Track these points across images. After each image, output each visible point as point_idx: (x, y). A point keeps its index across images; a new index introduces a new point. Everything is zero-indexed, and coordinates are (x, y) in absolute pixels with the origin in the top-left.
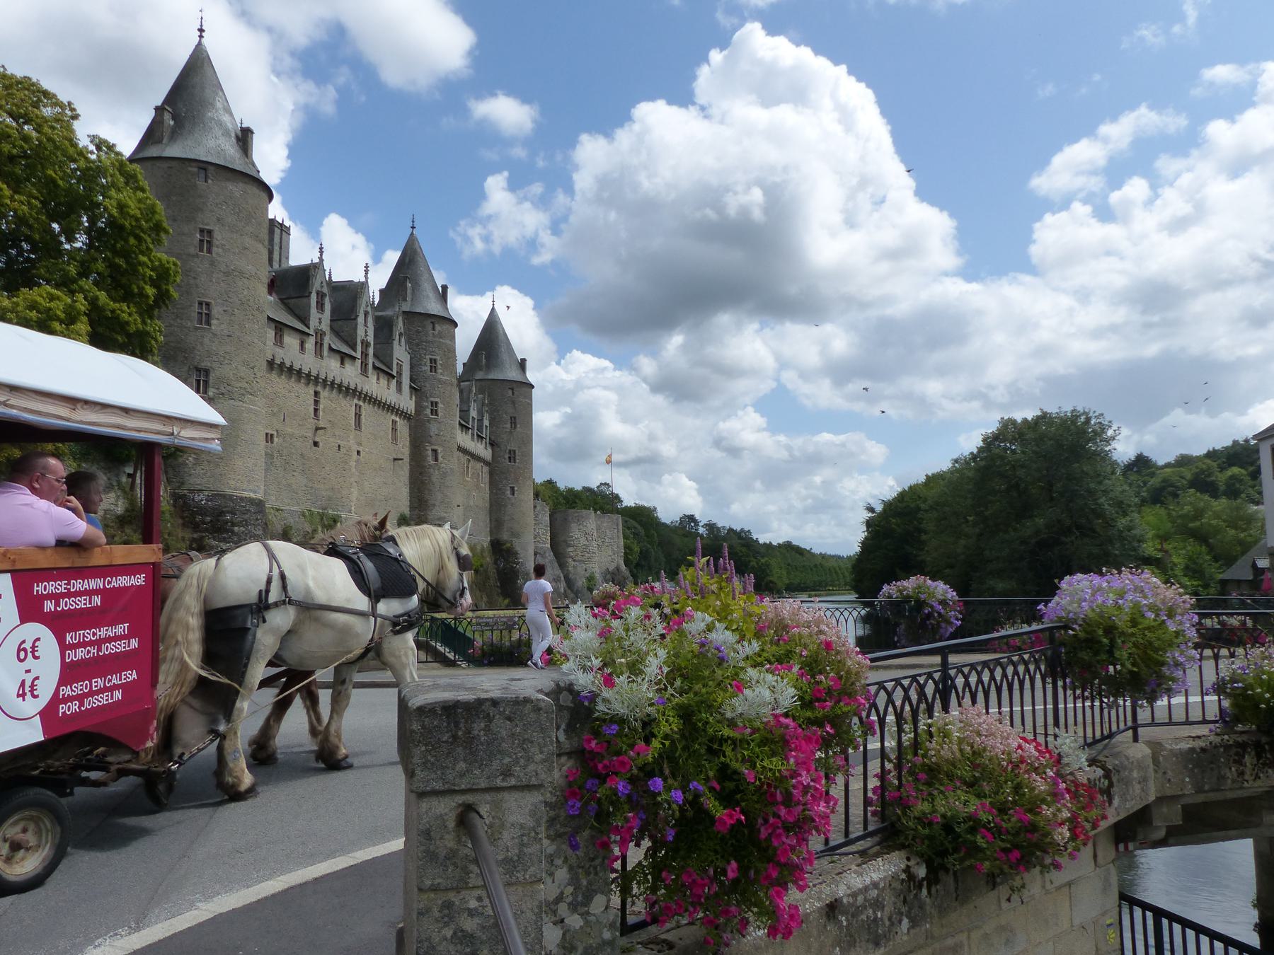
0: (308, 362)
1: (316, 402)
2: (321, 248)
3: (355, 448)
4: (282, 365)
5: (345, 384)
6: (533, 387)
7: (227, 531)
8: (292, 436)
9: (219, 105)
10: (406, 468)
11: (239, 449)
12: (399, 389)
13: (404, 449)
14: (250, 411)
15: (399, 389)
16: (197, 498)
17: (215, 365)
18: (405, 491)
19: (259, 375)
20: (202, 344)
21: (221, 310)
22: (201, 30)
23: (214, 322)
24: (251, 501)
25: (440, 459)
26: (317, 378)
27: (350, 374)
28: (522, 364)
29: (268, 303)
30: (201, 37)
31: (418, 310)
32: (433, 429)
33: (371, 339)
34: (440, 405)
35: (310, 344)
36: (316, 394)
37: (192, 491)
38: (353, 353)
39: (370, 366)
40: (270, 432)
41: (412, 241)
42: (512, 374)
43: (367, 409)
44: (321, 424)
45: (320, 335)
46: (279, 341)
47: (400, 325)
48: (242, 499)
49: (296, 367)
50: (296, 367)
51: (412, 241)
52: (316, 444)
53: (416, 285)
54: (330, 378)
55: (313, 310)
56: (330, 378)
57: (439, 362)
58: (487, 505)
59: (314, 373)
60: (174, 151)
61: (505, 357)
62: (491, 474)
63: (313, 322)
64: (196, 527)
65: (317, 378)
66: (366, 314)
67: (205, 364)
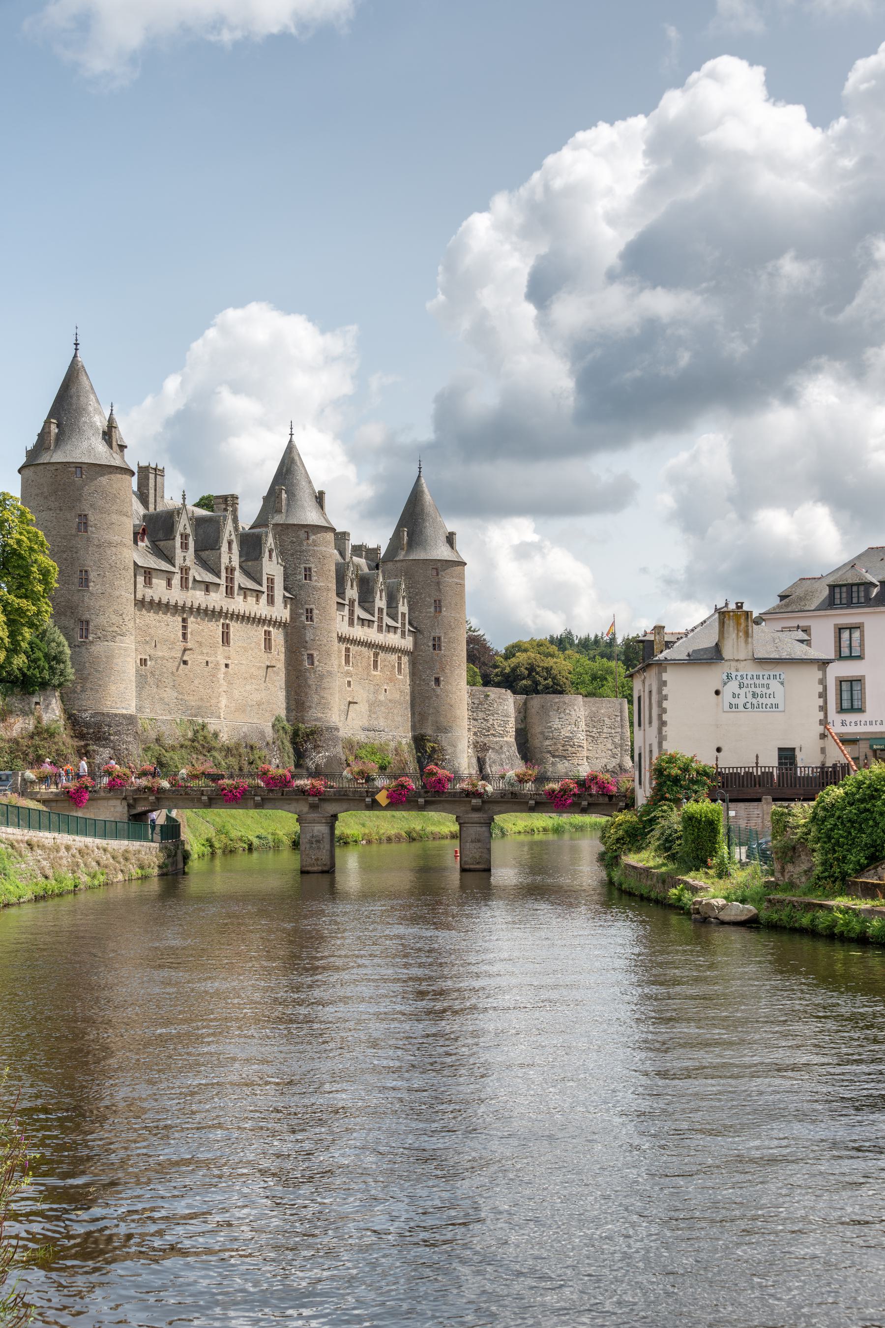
0: (176, 595)
1: (185, 627)
2: (184, 495)
4: (152, 601)
5: (211, 608)
6: (465, 564)
8: (163, 658)
9: (91, 409)
11: (113, 678)
12: (271, 601)
14: (120, 648)
15: (271, 601)
16: (84, 716)
17: (93, 617)
18: (281, 695)
19: (127, 619)
20: (83, 601)
21: (95, 574)
23: (92, 584)
24: (124, 716)
25: (316, 663)
27: (216, 599)
29: (140, 555)
30: (76, 349)
31: (291, 522)
32: (309, 636)
33: (236, 563)
34: (315, 611)
35: (176, 580)
36: (184, 620)
37: (79, 711)
38: (217, 580)
40: (144, 657)
42: (442, 552)
44: (189, 645)
45: (185, 570)
46: (148, 583)
47: (270, 542)
48: (116, 715)
49: (164, 601)
50: (164, 601)
52: (185, 663)
53: (291, 495)
55: (178, 551)
56: (196, 605)
57: (314, 570)
58: (408, 698)
59: (180, 603)
60: (58, 457)
61: (429, 531)
62: (413, 664)
63: (179, 561)
64: (81, 736)
65: (184, 607)
66: (230, 543)
67: (86, 616)
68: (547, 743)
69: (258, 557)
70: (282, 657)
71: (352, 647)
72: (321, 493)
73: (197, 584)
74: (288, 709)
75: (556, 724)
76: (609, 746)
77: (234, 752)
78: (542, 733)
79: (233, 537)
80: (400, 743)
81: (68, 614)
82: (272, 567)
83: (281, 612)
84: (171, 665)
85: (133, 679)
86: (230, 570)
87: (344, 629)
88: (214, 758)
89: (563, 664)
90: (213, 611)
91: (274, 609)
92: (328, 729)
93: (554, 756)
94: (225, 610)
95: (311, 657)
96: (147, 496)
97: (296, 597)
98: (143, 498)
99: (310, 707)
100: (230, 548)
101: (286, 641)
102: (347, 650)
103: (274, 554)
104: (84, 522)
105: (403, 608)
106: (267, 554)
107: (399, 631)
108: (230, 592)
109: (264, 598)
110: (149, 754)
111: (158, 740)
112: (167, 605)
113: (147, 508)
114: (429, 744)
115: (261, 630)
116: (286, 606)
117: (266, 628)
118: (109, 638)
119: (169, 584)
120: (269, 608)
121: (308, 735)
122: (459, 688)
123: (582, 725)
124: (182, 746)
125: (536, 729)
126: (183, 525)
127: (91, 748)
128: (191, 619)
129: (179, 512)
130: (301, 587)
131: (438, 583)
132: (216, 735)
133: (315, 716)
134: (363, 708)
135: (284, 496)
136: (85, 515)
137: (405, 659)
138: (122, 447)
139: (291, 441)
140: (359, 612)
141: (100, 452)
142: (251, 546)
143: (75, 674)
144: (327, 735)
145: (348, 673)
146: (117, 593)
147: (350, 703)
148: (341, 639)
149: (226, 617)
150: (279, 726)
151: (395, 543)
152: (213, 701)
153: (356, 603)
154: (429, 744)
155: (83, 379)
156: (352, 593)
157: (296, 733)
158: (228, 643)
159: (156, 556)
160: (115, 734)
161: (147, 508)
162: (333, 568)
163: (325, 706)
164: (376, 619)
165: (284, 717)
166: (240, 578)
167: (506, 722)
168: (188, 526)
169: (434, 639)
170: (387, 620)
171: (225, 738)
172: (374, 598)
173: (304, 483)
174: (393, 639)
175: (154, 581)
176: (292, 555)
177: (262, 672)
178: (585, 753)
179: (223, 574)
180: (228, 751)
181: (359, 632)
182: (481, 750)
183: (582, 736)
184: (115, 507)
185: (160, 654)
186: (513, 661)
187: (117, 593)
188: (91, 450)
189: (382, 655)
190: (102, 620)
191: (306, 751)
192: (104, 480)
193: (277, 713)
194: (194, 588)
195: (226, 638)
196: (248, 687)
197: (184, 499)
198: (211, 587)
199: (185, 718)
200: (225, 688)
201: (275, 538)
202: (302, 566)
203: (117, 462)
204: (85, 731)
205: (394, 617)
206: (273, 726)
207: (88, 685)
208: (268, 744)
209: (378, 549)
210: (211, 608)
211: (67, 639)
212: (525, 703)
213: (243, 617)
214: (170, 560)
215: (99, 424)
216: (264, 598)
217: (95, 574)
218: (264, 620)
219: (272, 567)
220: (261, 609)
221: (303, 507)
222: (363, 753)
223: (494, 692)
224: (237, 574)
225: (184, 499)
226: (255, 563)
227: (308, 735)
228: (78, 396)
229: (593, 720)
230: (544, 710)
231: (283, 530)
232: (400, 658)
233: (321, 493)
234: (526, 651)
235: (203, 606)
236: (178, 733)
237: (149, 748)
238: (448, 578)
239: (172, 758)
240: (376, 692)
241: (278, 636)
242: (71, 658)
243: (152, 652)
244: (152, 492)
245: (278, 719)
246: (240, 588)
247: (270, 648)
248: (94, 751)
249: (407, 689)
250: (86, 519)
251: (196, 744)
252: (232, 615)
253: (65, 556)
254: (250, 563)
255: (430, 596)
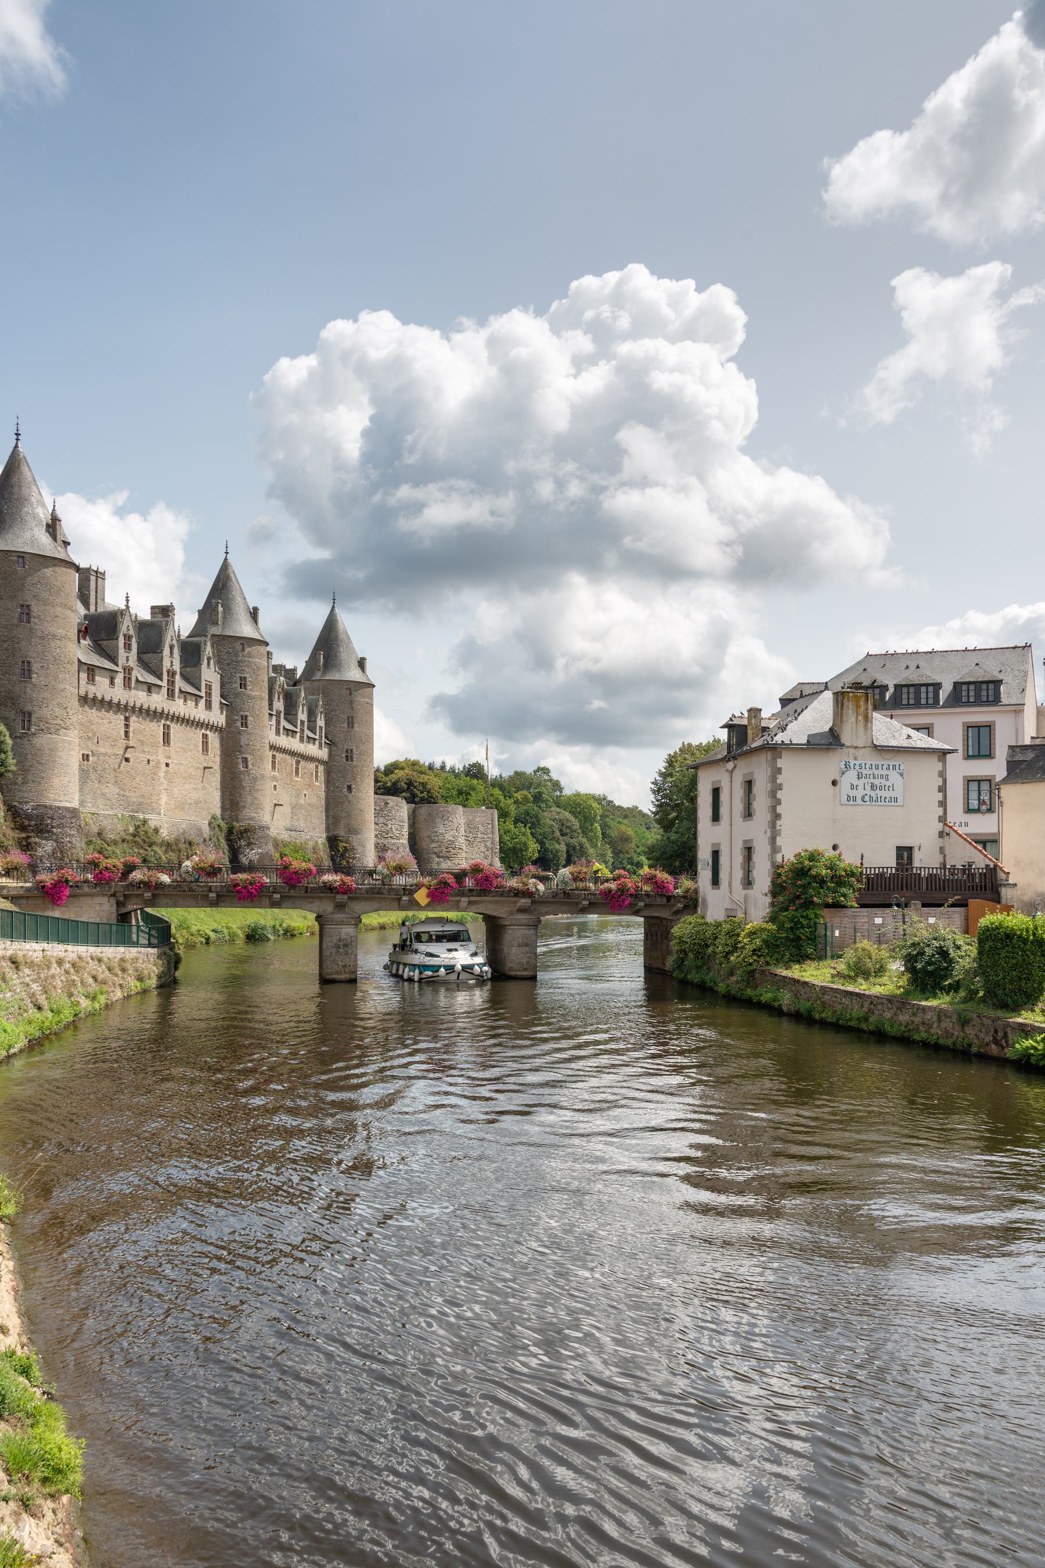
0: (118, 693)
1: (127, 726)
3: (164, 761)
4: (95, 699)
5: (153, 708)
7: (49, 832)
8: (105, 754)
9: (33, 500)
10: (218, 776)
11: (56, 771)
12: (209, 706)
13: (215, 757)
14: (64, 741)
15: (209, 706)
16: (25, 808)
17: (36, 708)
18: (217, 795)
19: (71, 713)
22: (17, 434)
23: (34, 676)
24: (67, 809)
25: (250, 766)
26: (126, 706)
27: (157, 701)
28: (362, 663)
29: (82, 651)
32: (244, 740)
33: (177, 667)
34: (250, 718)
35: (119, 679)
36: (127, 719)
37: (20, 803)
38: (159, 682)
39: (177, 691)
40: (86, 753)
41: (225, 566)
42: (354, 674)
43: (175, 729)
44: (131, 743)
45: (128, 670)
46: (91, 679)
47: (208, 650)
48: (59, 808)
51: (225, 566)
52: (127, 760)
54: (138, 705)
55: (121, 650)
56: (138, 705)
58: (323, 802)
61: (343, 655)
62: (328, 773)
63: (122, 661)
64: (23, 828)
65: (126, 706)
66: (171, 647)
67: (29, 708)
68: (434, 845)
69: (198, 663)
70: (218, 759)
71: (277, 754)
72: (256, 609)
73: (140, 685)
74: (223, 808)
75: (441, 829)
76: (483, 849)
77: (174, 847)
78: (429, 837)
79: (175, 642)
80: (317, 842)
81: (9, 704)
82: (210, 674)
83: (218, 717)
84: (114, 762)
85: (77, 772)
86: (172, 674)
87: (272, 737)
88: (155, 852)
89: (434, 783)
90: (155, 712)
91: (212, 714)
92: (260, 827)
93: (439, 857)
94: (166, 712)
95: (245, 761)
96: (88, 597)
97: (230, 705)
98: (84, 599)
99: (244, 807)
100: (171, 653)
101: (222, 745)
102: (274, 757)
103: (212, 662)
104: (26, 612)
105: (321, 722)
106: (205, 661)
107: (317, 742)
108: (171, 694)
109: (202, 702)
110: (91, 847)
111: (99, 834)
112: (110, 702)
113: (88, 608)
114: (341, 844)
115: (200, 732)
116: (222, 713)
117: (203, 731)
118: (52, 731)
119: (112, 683)
120: (207, 713)
121: (242, 833)
122: (367, 796)
123: (462, 830)
124: (123, 841)
125: (424, 834)
126: (125, 627)
127: (33, 840)
128: (133, 718)
129: (122, 613)
130: (237, 695)
131: (351, 702)
132: (156, 830)
133: (249, 815)
134: (288, 812)
135: (220, 609)
136: (28, 606)
137: (321, 768)
138: (66, 544)
139: (226, 559)
140: (284, 723)
141: (44, 544)
142: (191, 652)
143: (16, 765)
144: (259, 833)
145: (274, 778)
146: (61, 686)
147: (276, 805)
148: (272, 747)
149: (167, 719)
150: (215, 824)
151: (312, 665)
152: (154, 798)
153: (282, 715)
154: (341, 844)
155: (24, 469)
156: (279, 705)
157: (230, 831)
158: (169, 743)
159: (99, 655)
160: (58, 827)
161: (88, 608)
162: (266, 679)
163: (259, 807)
164: (298, 730)
165: (219, 816)
166: (179, 683)
167: (402, 827)
168: (131, 627)
169: (347, 751)
170: (307, 732)
171: (164, 833)
172: (297, 711)
173: (239, 599)
174: (312, 750)
175: (97, 678)
176: (228, 664)
177: (200, 773)
178: (464, 855)
179: (165, 677)
180: (168, 846)
181: (284, 741)
182: (381, 849)
183: (462, 840)
184: (59, 600)
185: (103, 750)
186: (393, 777)
187: (61, 686)
188: (33, 541)
189: (302, 763)
190: (45, 712)
191: (240, 847)
192: (48, 572)
193: (213, 812)
194: (136, 689)
195: (166, 739)
196: (187, 787)
197: (127, 601)
198: (153, 689)
199: (127, 814)
200: (165, 786)
201: (213, 647)
202: (238, 675)
203: (62, 556)
204: (26, 823)
205: (312, 729)
206: (210, 824)
207: (30, 777)
208: (205, 840)
209: (295, 670)
210: (153, 708)
211: (8, 729)
212: (414, 811)
213: (183, 719)
214: (114, 660)
215: (42, 516)
216: (202, 702)
217: (38, 665)
218: (203, 724)
219: (210, 674)
220: (199, 712)
221: (238, 620)
222: (287, 851)
223: (392, 800)
224: (178, 677)
225: (127, 601)
226: (194, 669)
227: (242, 833)
228: (20, 487)
229: (470, 826)
230: (431, 818)
231: (220, 640)
232: (317, 767)
233: (256, 609)
234: (402, 768)
235: (145, 707)
236: (120, 827)
237: (91, 841)
238: (359, 698)
239: (114, 852)
240: (297, 796)
241: (214, 739)
242: (12, 749)
243: (94, 748)
244: (93, 593)
245: (214, 817)
246: (181, 691)
247: (207, 751)
248: (36, 843)
249: (323, 795)
250: (29, 610)
251: (137, 839)
252: (173, 717)
253: (5, 646)
254: (188, 669)
255: (343, 713)
